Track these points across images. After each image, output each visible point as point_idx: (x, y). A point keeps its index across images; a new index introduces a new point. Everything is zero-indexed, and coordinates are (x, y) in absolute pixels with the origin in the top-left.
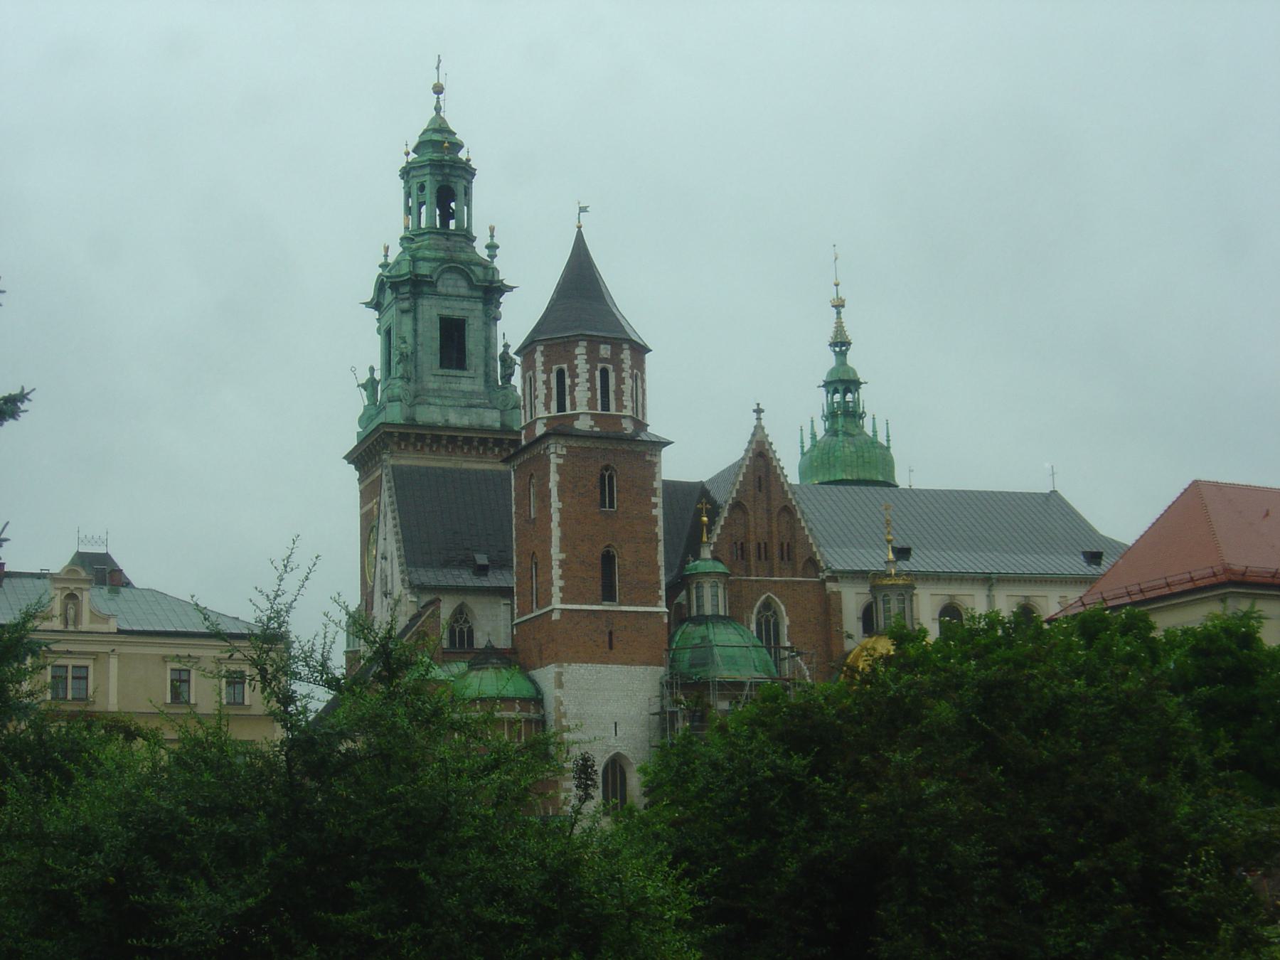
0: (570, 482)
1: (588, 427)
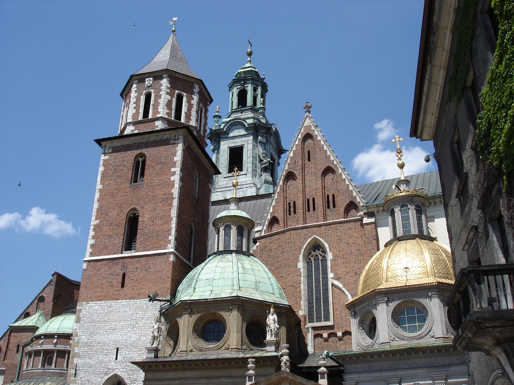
1: (130, 131)
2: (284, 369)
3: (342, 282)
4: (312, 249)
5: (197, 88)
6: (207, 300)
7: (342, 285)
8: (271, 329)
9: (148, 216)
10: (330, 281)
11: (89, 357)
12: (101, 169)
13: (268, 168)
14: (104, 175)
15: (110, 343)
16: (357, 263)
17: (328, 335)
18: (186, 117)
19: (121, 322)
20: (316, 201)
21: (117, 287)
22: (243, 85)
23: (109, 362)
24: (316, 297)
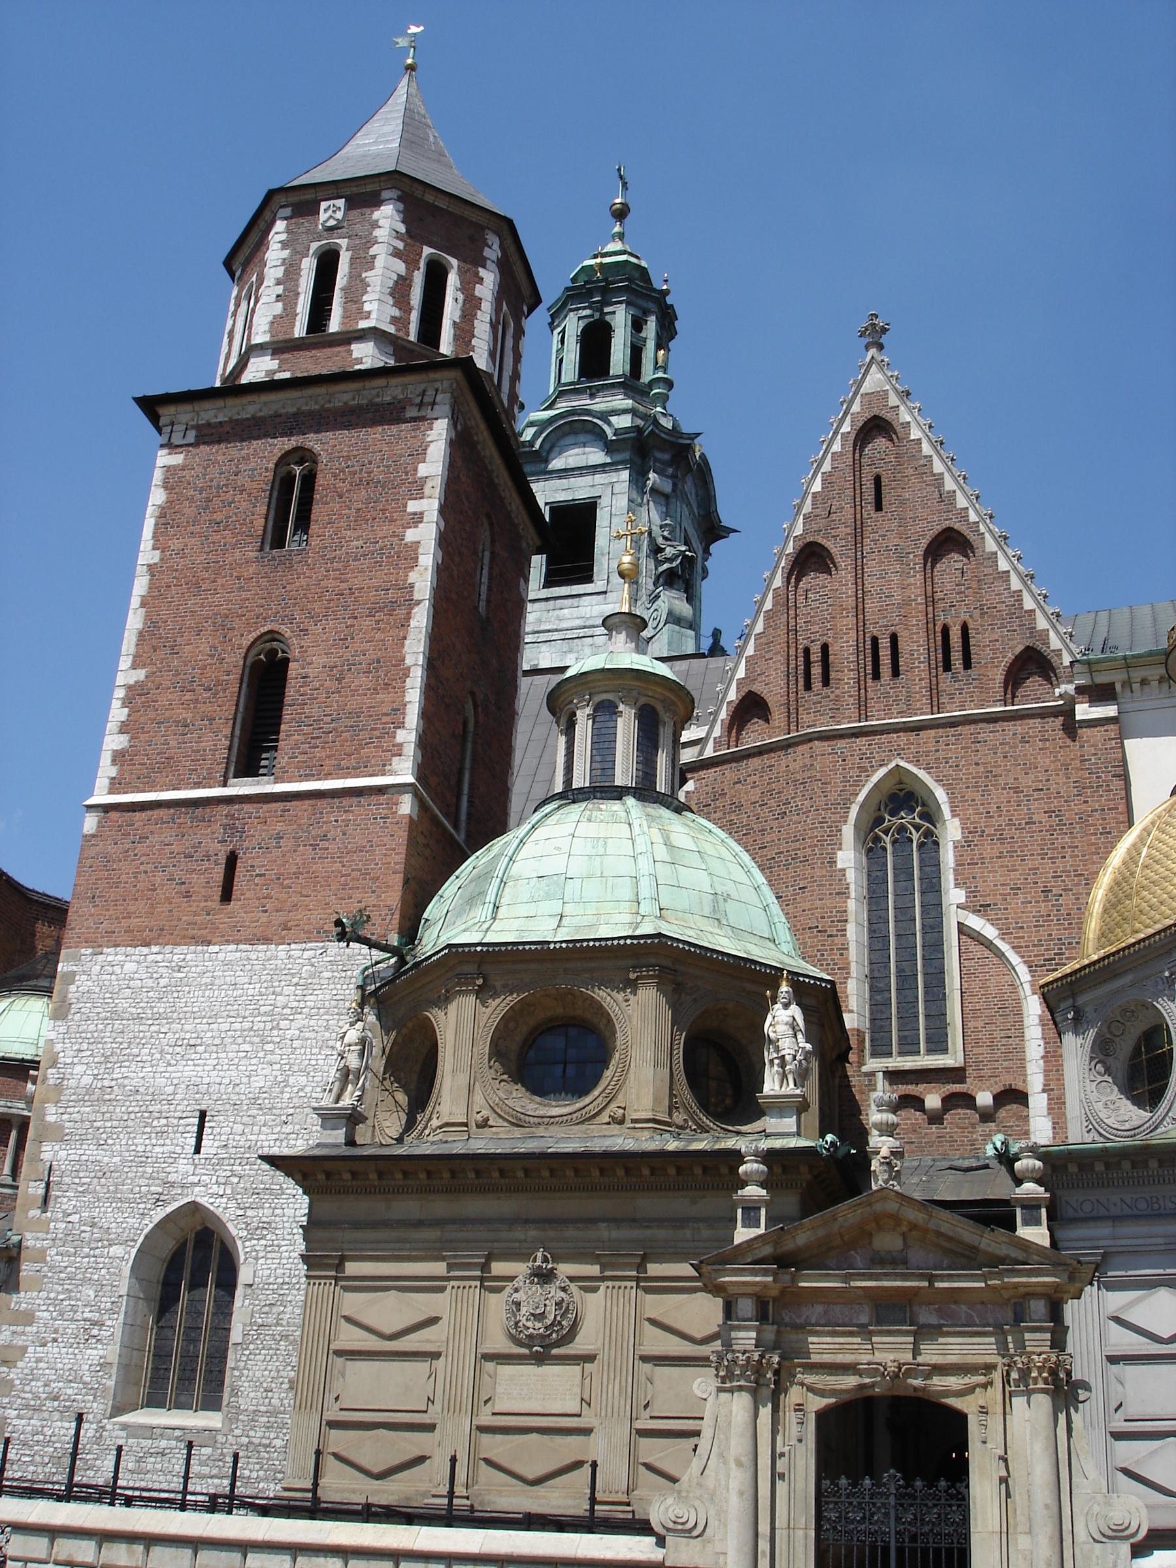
0: (192, 500)
2: (880, 1182)
3: (997, 919)
4: (886, 806)
5: (494, 247)
6: (546, 947)
7: (997, 932)
8: (783, 1056)
9: (322, 660)
10: (952, 918)
11: (98, 1139)
12: (157, 497)
13: (679, 577)
14: (165, 518)
15: (175, 1094)
16: (1049, 859)
17: (943, 1100)
18: (456, 338)
19: (219, 1020)
20: (903, 646)
21: (206, 901)
22: (599, 307)
23: (171, 1160)
24: (899, 970)
